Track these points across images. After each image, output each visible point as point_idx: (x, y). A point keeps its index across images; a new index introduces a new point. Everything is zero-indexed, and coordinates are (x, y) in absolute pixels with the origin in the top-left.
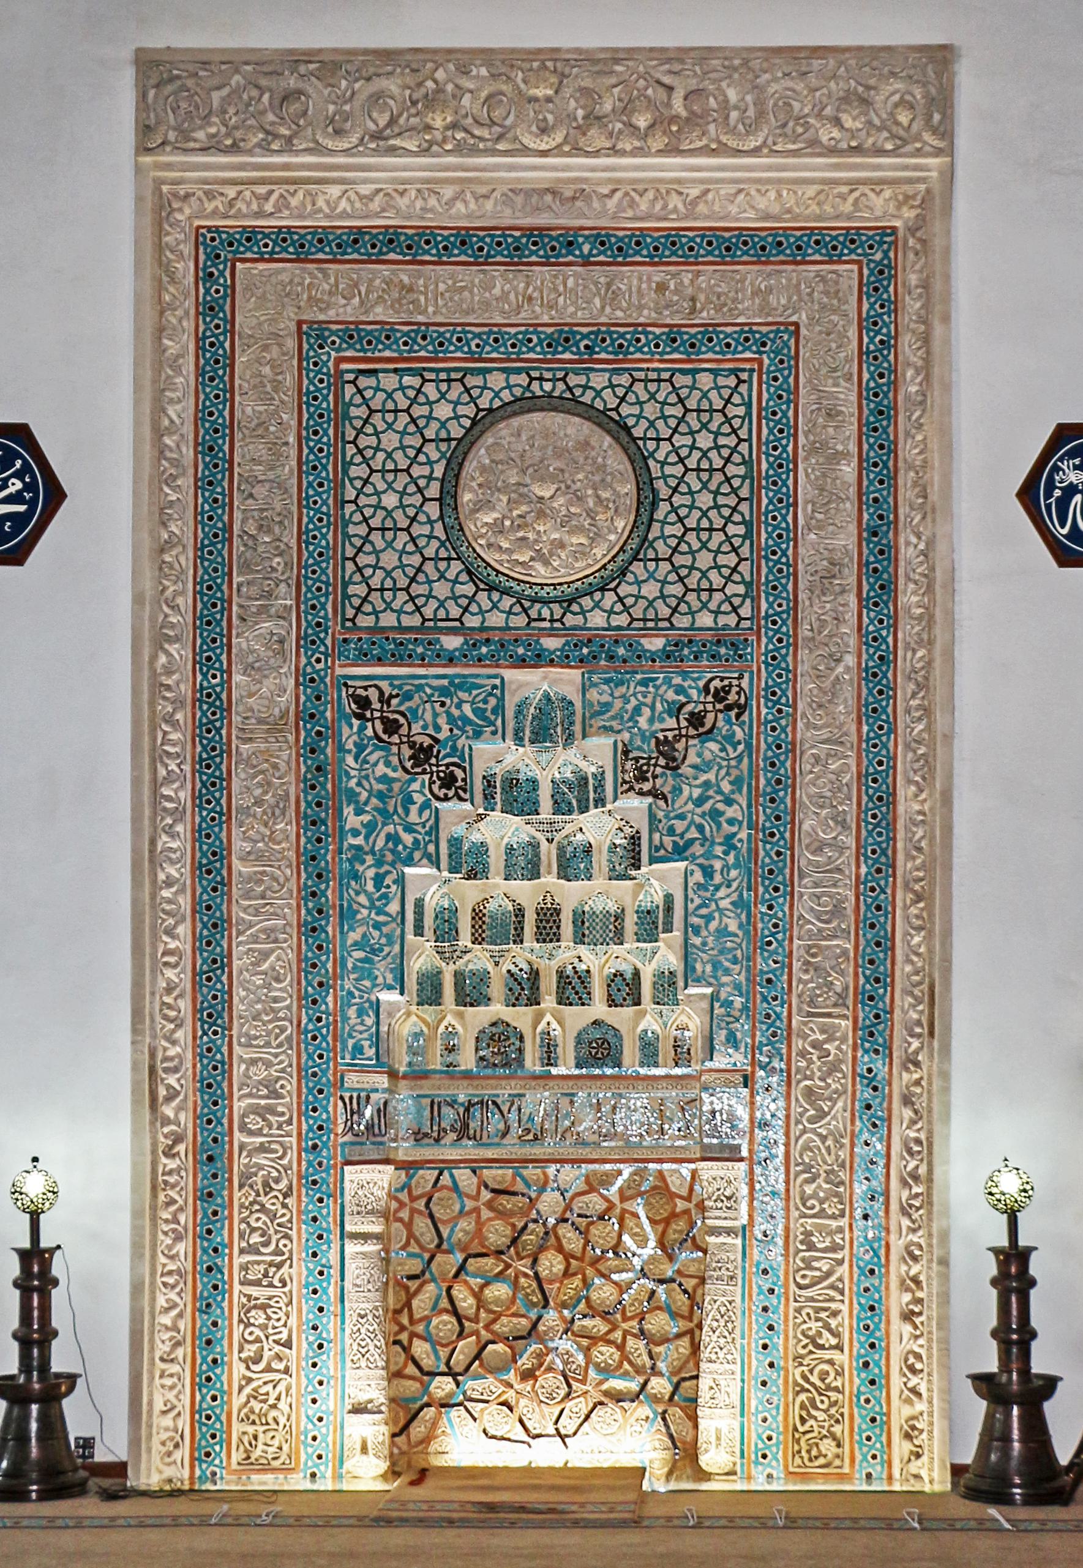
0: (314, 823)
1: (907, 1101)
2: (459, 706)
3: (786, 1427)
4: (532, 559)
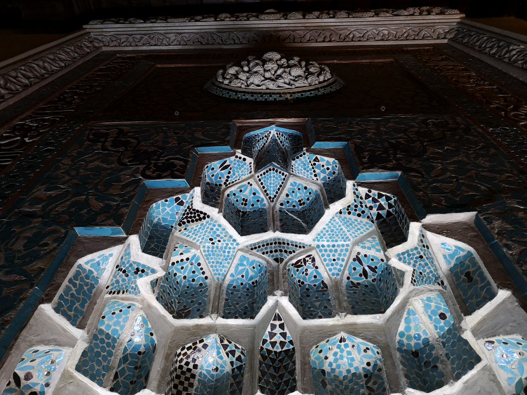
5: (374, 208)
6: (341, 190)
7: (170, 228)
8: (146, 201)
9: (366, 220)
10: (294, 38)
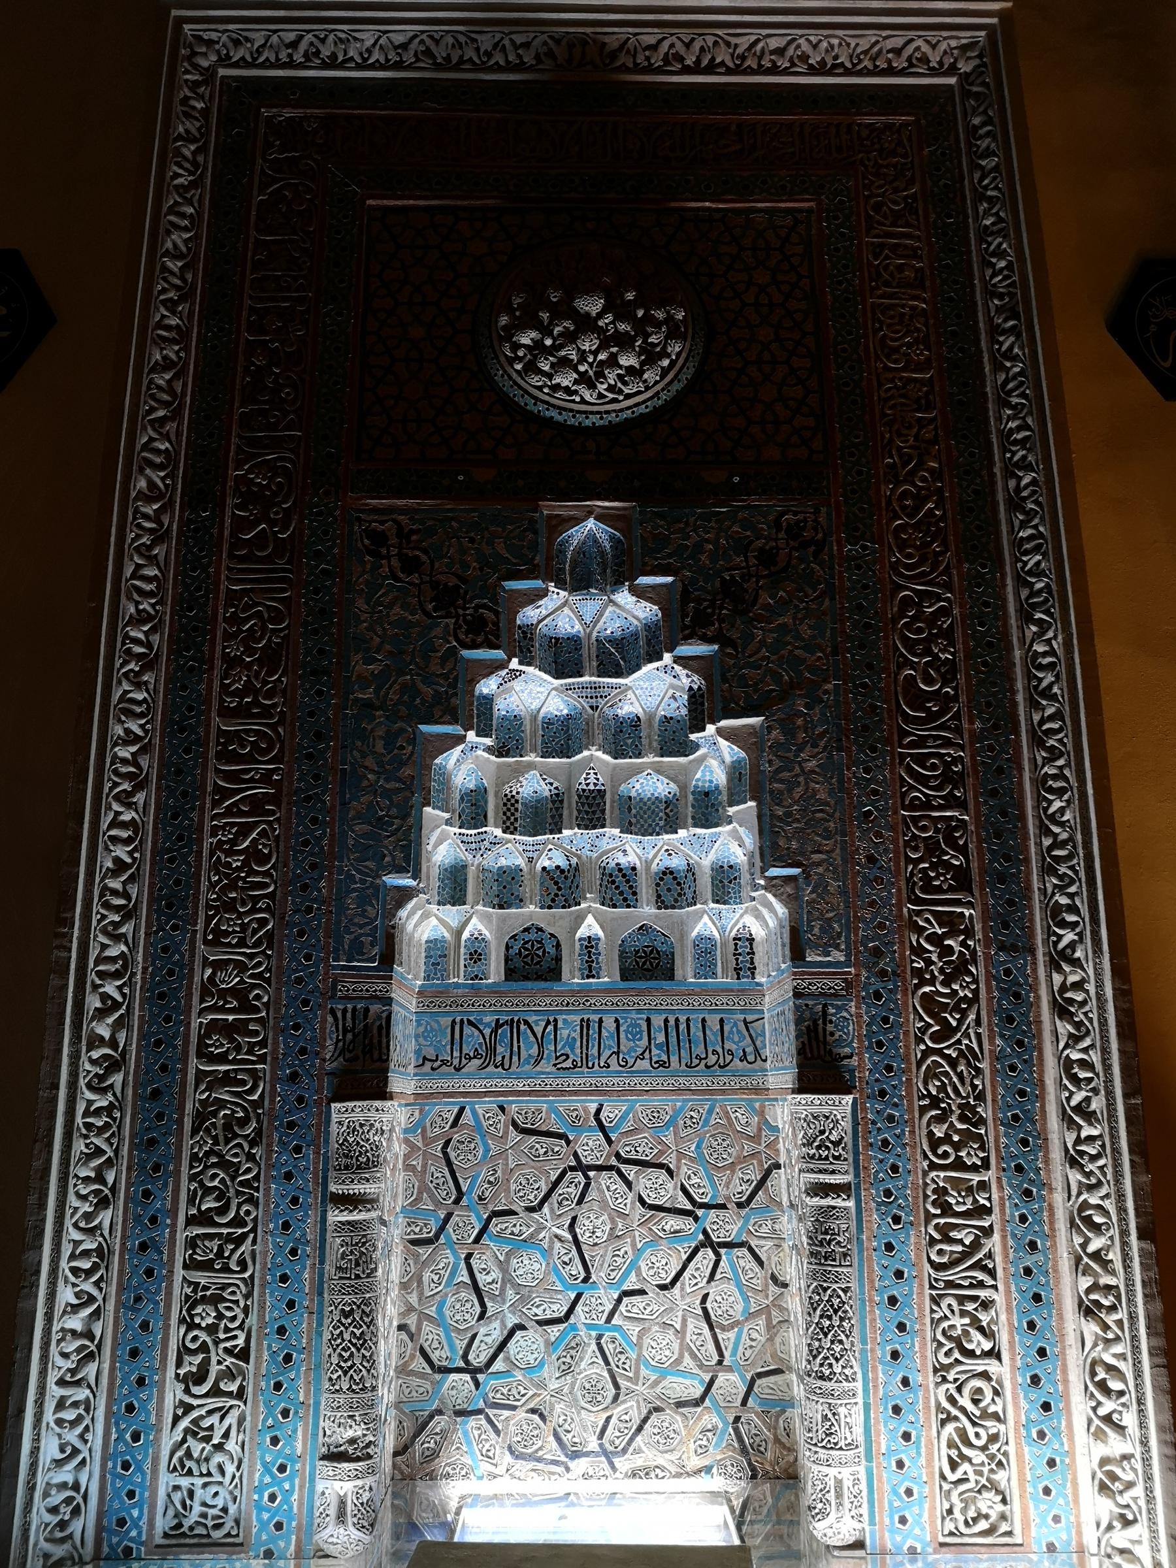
0: (314, 673)
1: (1062, 1010)
3: (931, 1474)
4: (576, 382)
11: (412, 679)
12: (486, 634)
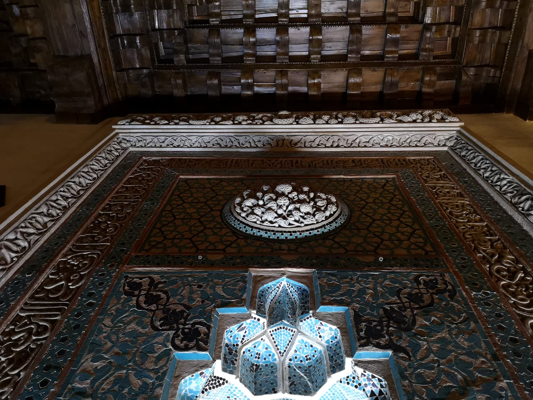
2: (213, 288)
5: (368, 386)
6: (341, 359)
7: (195, 398)
8: (176, 377)
9: (361, 392)
10: (305, 142)
11: (127, 373)
12: (198, 341)
